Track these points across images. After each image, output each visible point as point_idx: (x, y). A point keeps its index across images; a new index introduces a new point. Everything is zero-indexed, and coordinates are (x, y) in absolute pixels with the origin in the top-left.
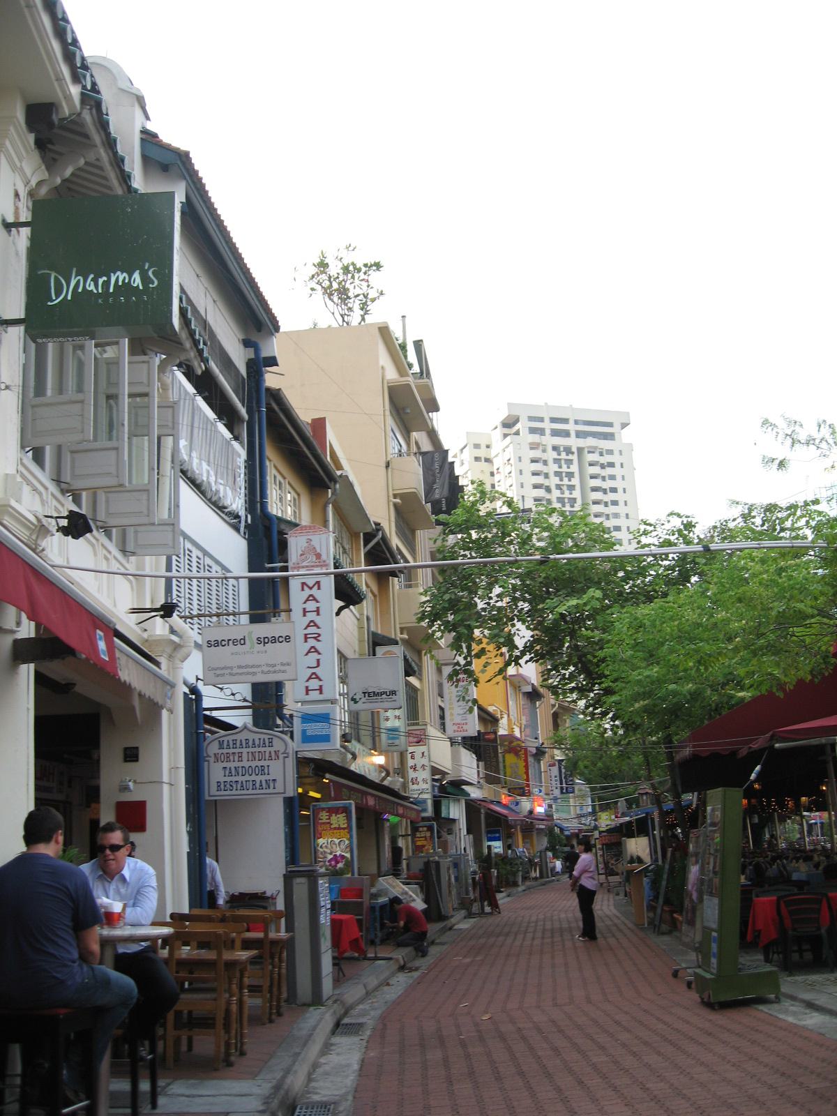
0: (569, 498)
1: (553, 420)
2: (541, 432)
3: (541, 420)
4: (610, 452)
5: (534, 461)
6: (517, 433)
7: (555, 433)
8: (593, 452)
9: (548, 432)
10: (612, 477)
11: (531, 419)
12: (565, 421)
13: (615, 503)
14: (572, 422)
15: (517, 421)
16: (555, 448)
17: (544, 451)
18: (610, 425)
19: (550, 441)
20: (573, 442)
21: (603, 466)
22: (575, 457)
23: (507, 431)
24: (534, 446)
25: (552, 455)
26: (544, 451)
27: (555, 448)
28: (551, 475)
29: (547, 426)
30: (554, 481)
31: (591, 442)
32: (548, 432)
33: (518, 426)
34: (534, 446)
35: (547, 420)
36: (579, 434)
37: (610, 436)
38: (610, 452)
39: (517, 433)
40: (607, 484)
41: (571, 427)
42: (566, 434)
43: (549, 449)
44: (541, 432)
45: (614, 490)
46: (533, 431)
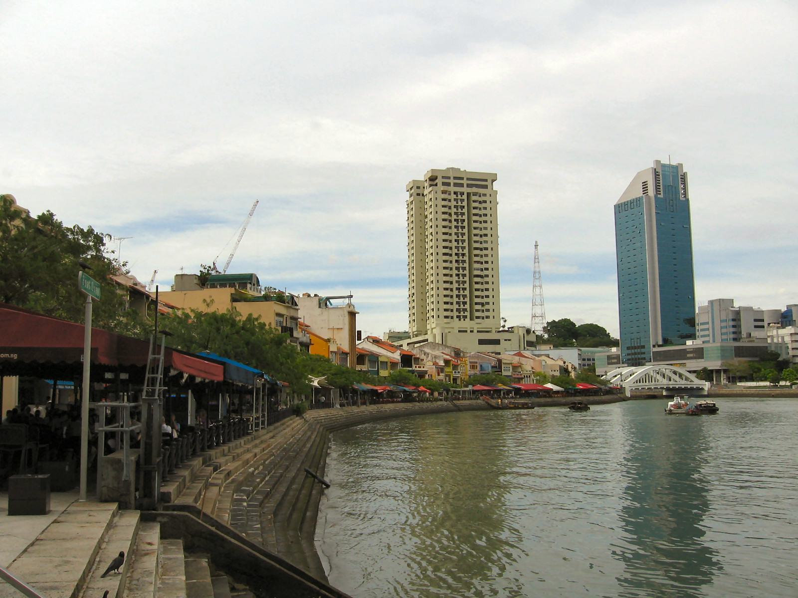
0: (461, 220)
1: (455, 178)
2: (448, 184)
3: (449, 178)
4: (485, 195)
5: (443, 200)
6: (436, 185)
7: (456, 185)
8: (476, 195)
9: (452, 184)
10: (485, 208)
11: (443, 177)
12: (462, 179)
13: (485, 222)
14: (465, 179)
15: (436, 178)
16: (455, 193)
17: (450, 194)
18: (486, 180)
19: (452, 189)
20: (465, 190)
21: (480, 202)
22: (465, 197)
23: (431, 183)
24: (444, 192)
25: (453, 196)
26: (450, 194)
27: (455, 193)
28: (453, 207)
29: (452, 181)
30: (454, 210)
31: (474, 190)
32: (452, 184)
33: (437, 181)
34: (444, 192)
35: (452, 178)
36: (468, 186)
37: (486, 187)
38: (485, 195)
39: (436, 185)
40: (482, 212)
41: (465, 182)
42: (462, 185)
43: (452, 193)
44: (448, 184)
45: (486, 215)
46: (444, 184)
